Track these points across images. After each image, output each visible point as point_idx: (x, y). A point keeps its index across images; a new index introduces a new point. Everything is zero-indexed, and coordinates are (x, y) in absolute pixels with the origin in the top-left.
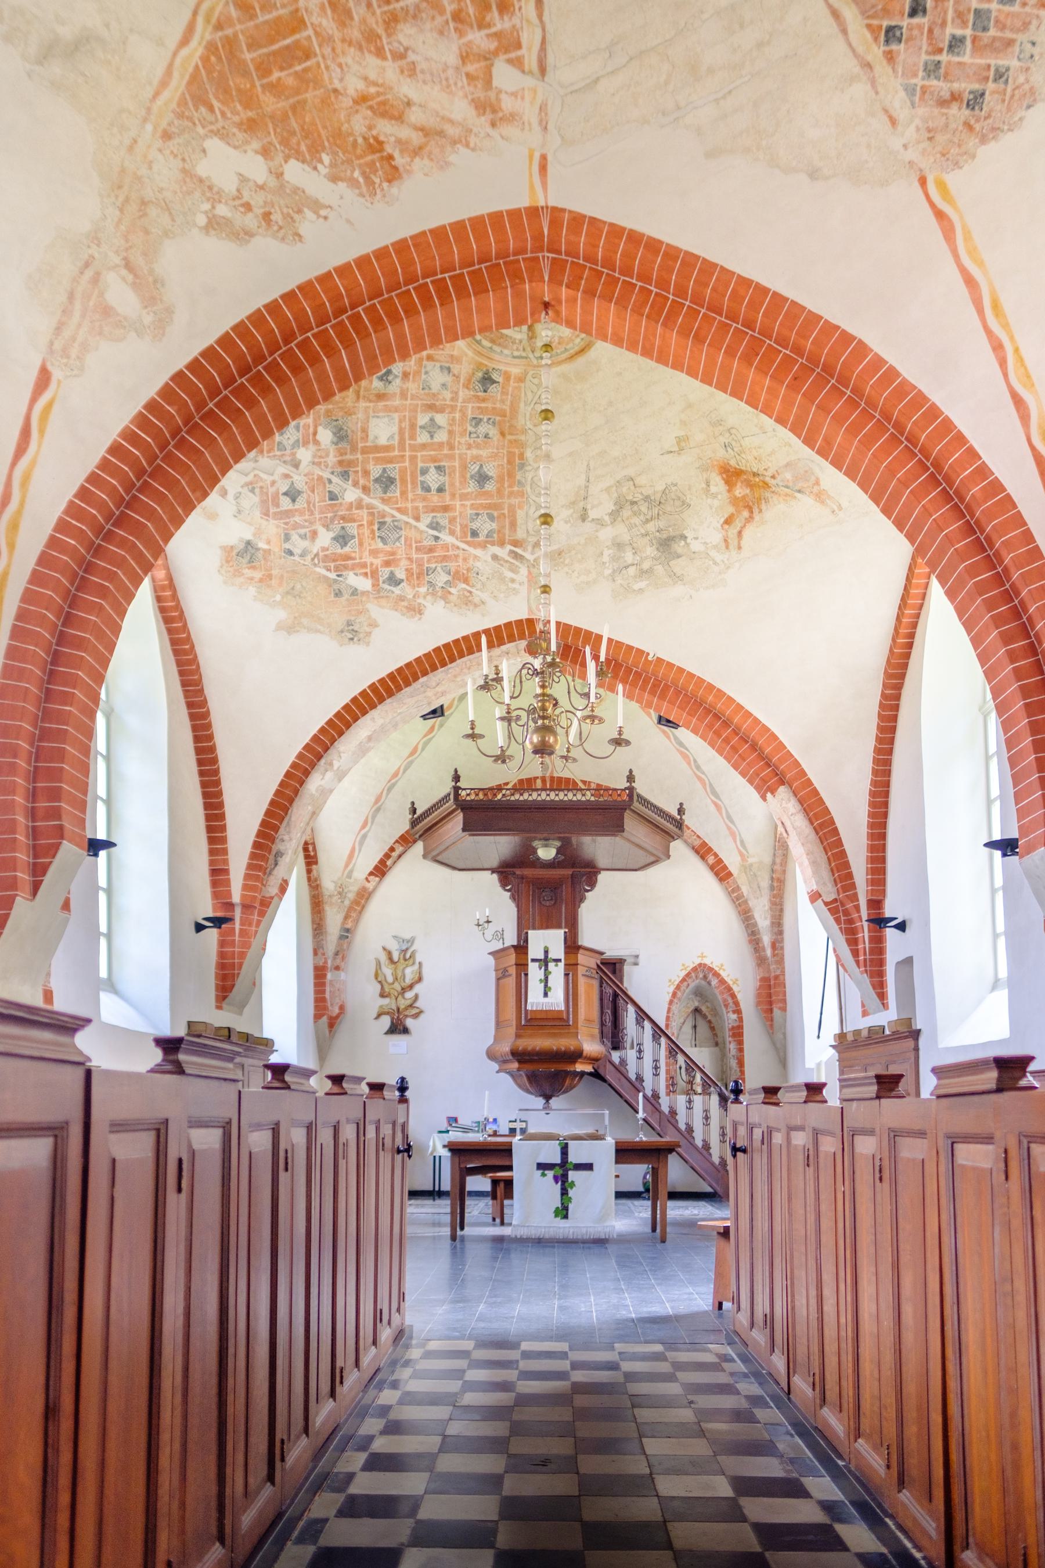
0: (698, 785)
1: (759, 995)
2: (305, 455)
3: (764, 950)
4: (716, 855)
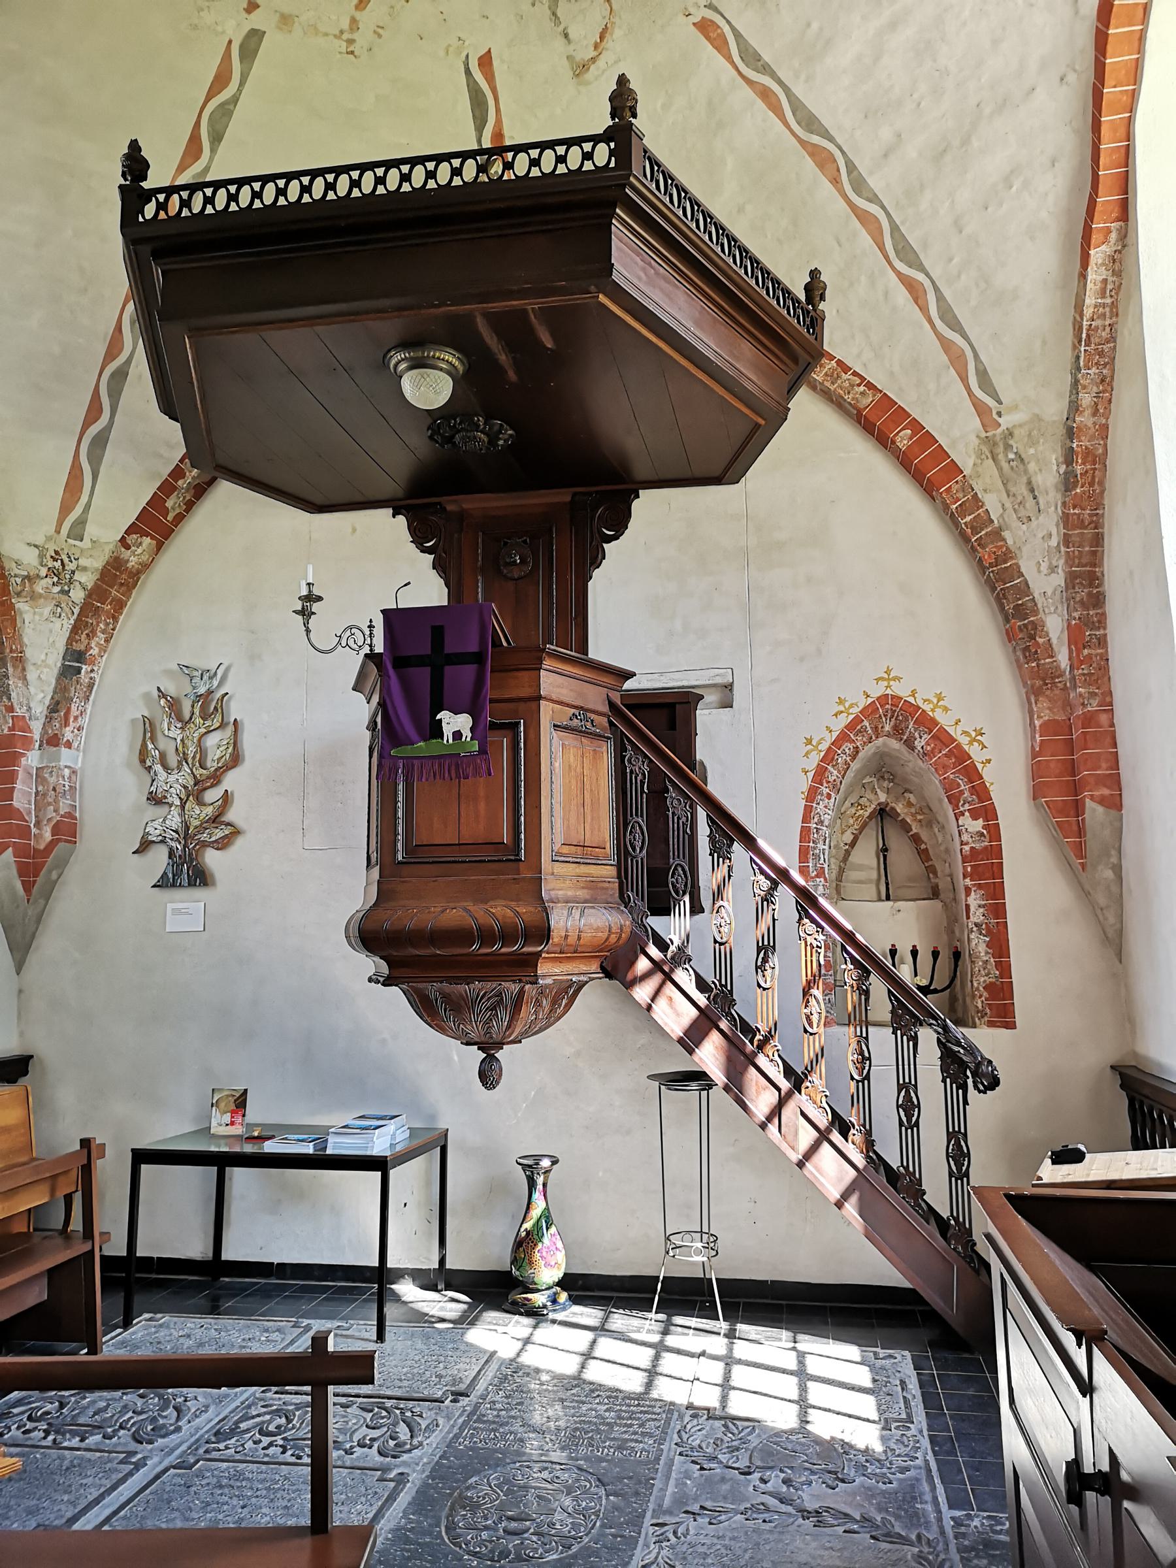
0: (865, 239)
1: (1037, 771)
3: (1050, 650)
4: (916, 426)
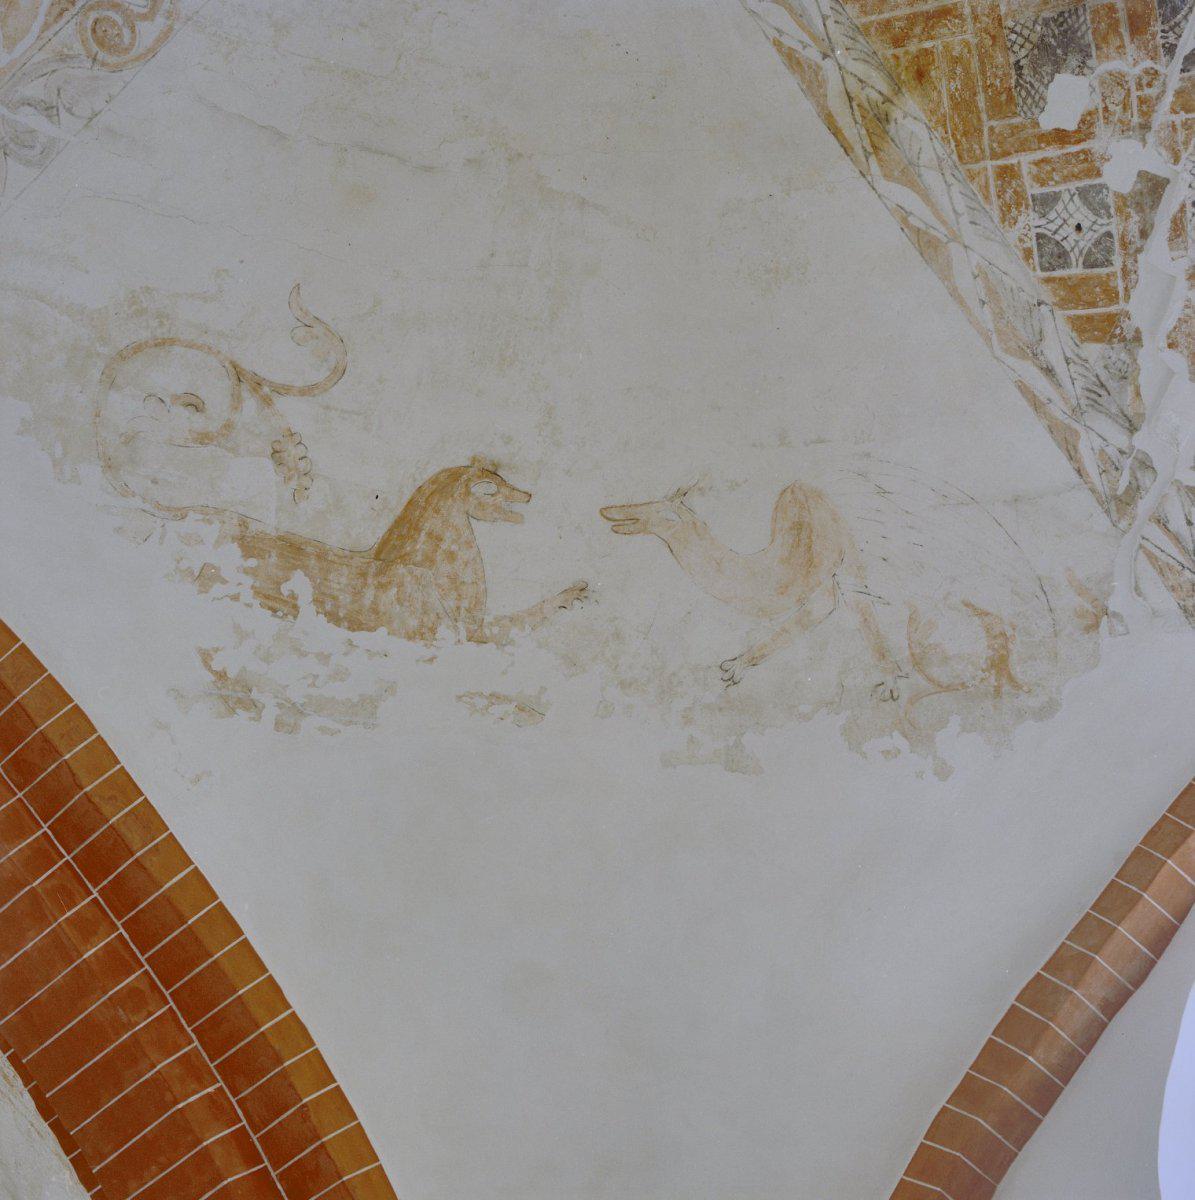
2: (1124, 162)
